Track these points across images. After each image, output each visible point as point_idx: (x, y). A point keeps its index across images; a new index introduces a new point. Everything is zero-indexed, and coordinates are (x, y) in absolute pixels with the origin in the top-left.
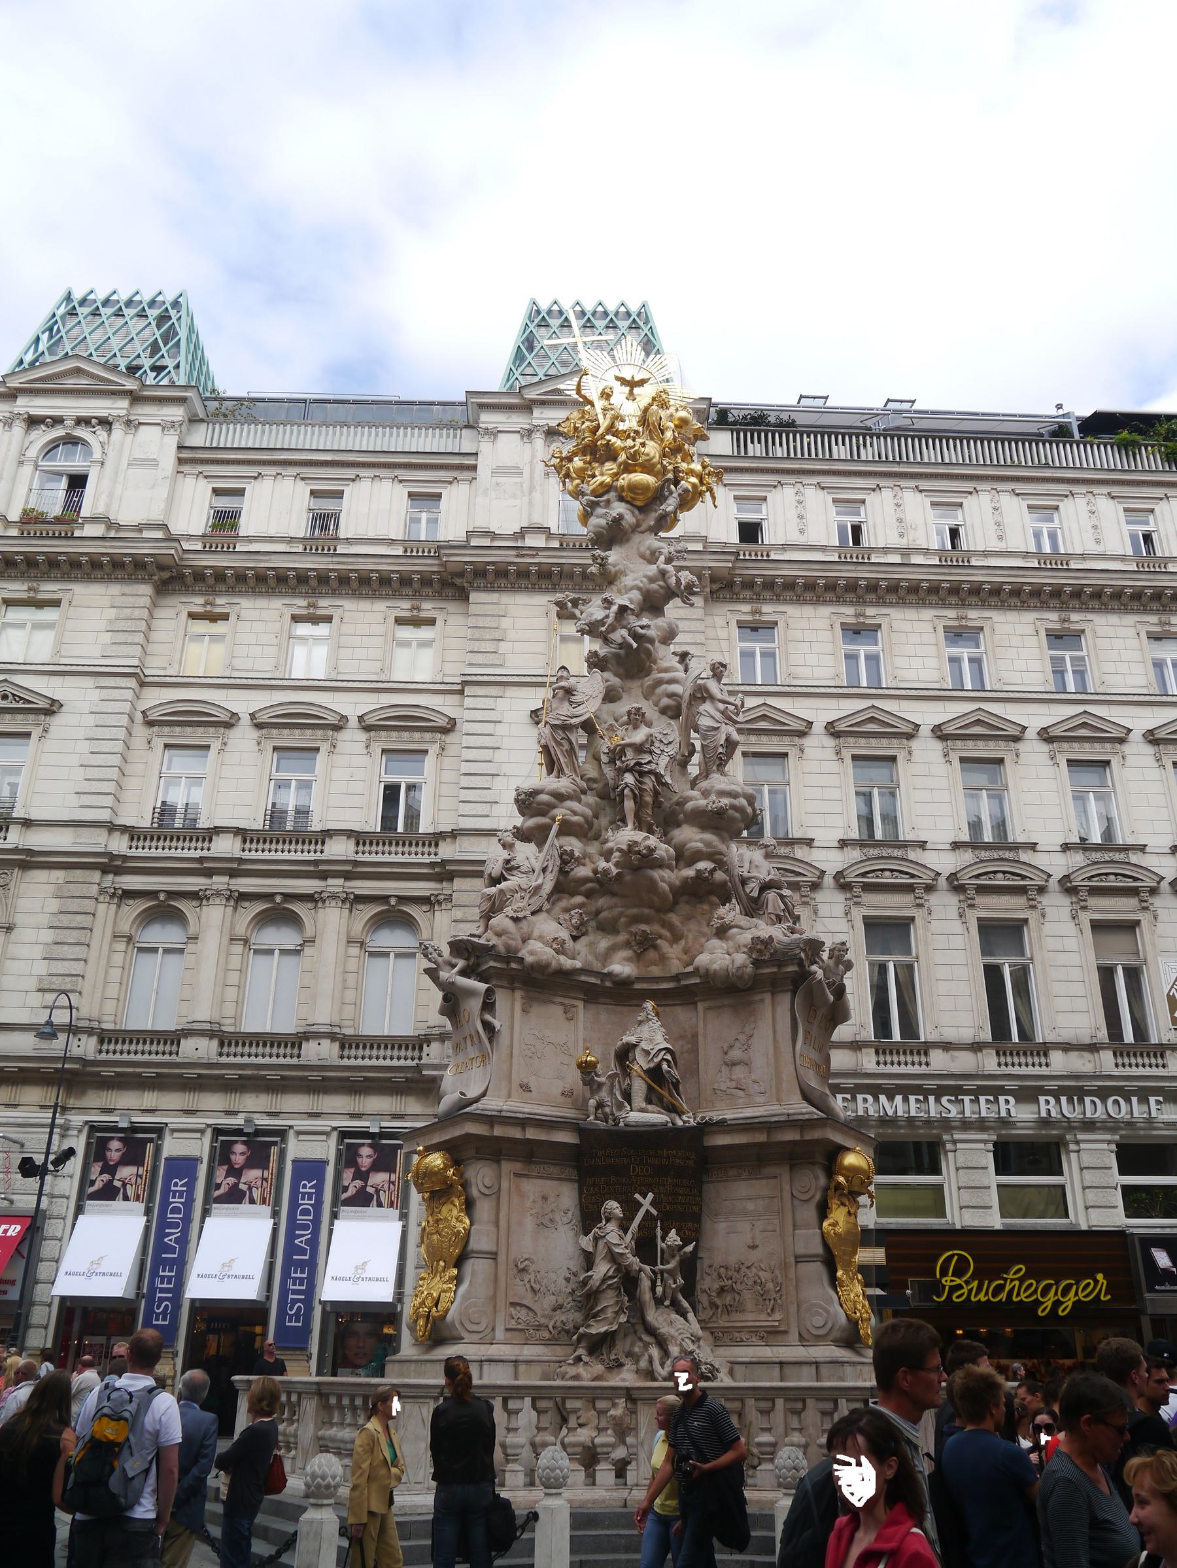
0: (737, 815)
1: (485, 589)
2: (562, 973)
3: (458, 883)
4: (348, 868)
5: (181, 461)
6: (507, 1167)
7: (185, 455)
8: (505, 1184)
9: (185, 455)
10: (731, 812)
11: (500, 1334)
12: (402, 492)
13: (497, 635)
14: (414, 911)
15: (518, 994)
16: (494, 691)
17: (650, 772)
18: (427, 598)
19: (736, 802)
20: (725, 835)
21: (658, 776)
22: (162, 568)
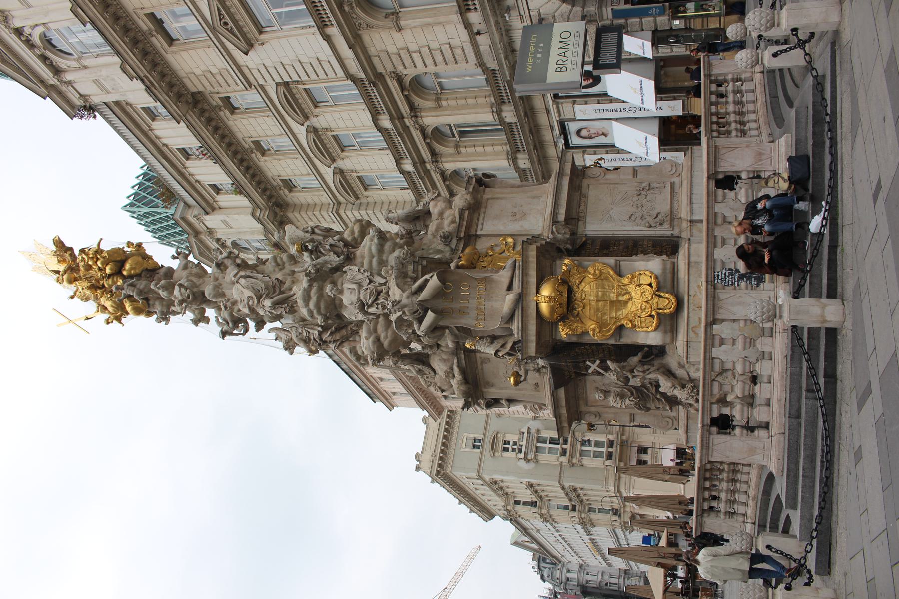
0: (322, 306)
1: (184, 86)
2: (463, 372)
3: (380, 69)
4: (396, 121)
5: (214, 209)
6: (583, 408)
7: (209, 210)
8: (593, 409)
9: (209, 210)
10: (323, 311)
11: (674, 414)
12: (154, 125)
13: (209, 76)
14: (407, 80)
15: (485, 390)
16: (246, 71)
17: (321, 340)
18: (209, 104)
19: (315, 312)
20: (337, 302)
21: (320, 334)
22: (276, 214)
